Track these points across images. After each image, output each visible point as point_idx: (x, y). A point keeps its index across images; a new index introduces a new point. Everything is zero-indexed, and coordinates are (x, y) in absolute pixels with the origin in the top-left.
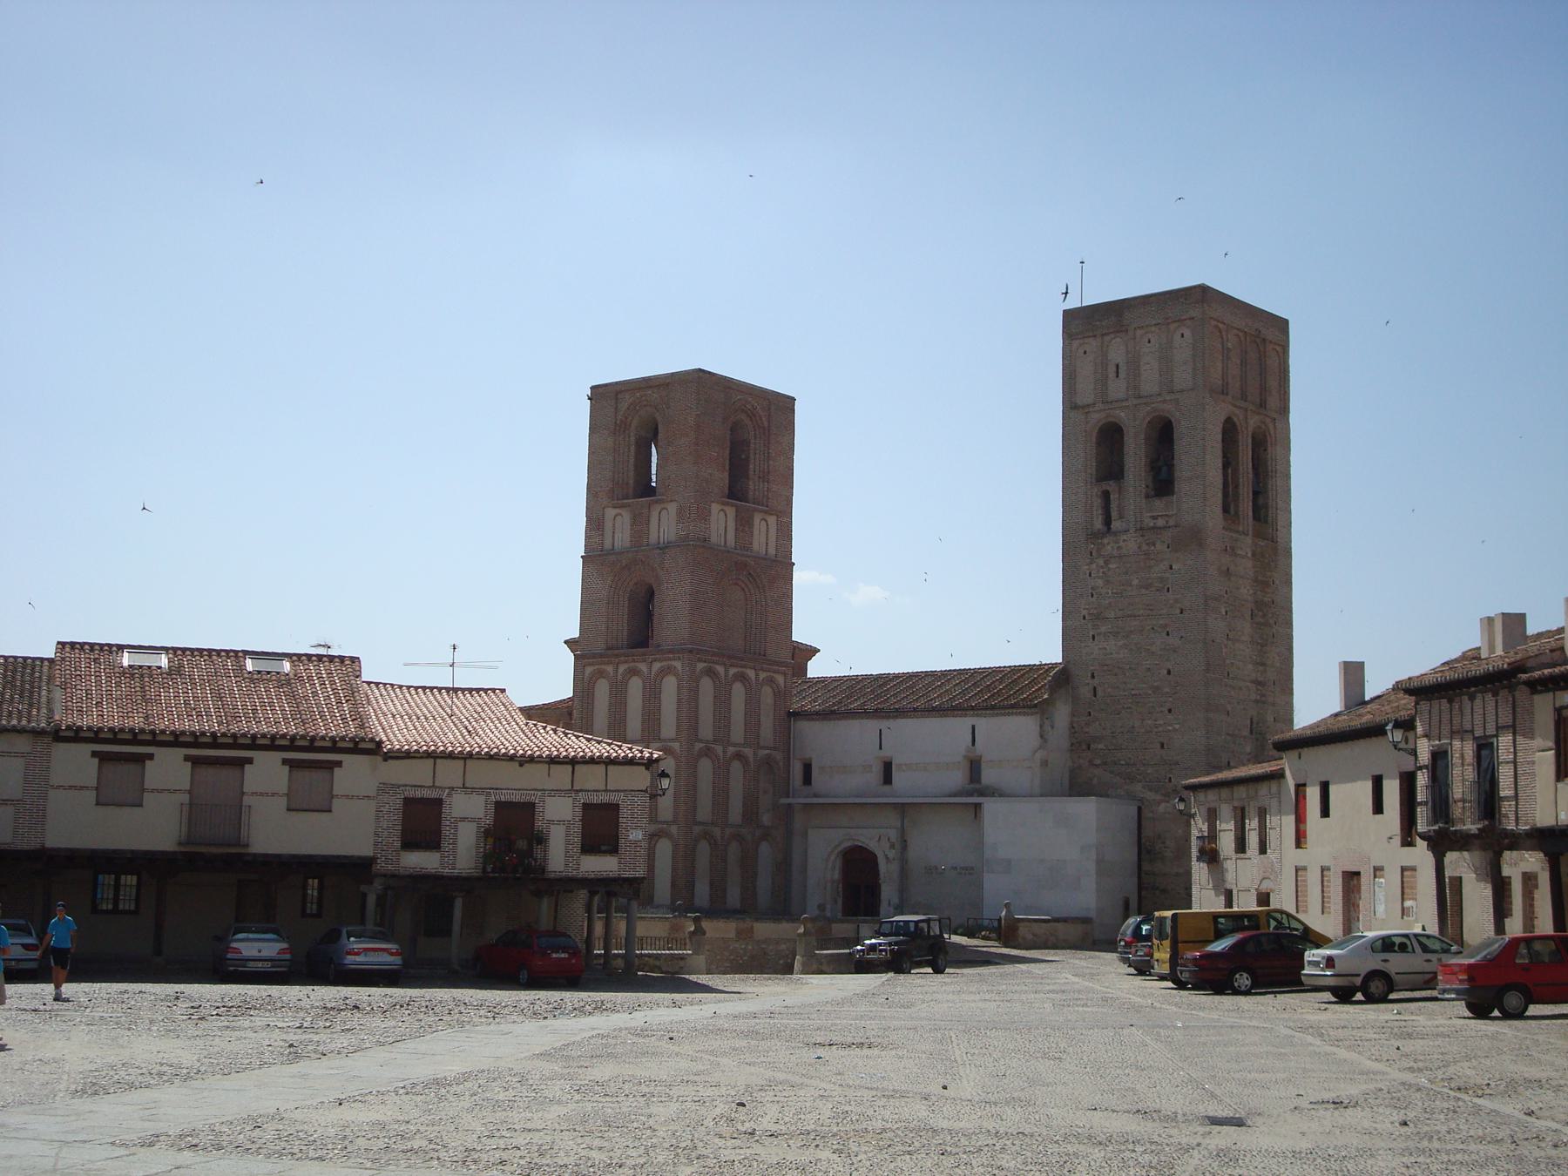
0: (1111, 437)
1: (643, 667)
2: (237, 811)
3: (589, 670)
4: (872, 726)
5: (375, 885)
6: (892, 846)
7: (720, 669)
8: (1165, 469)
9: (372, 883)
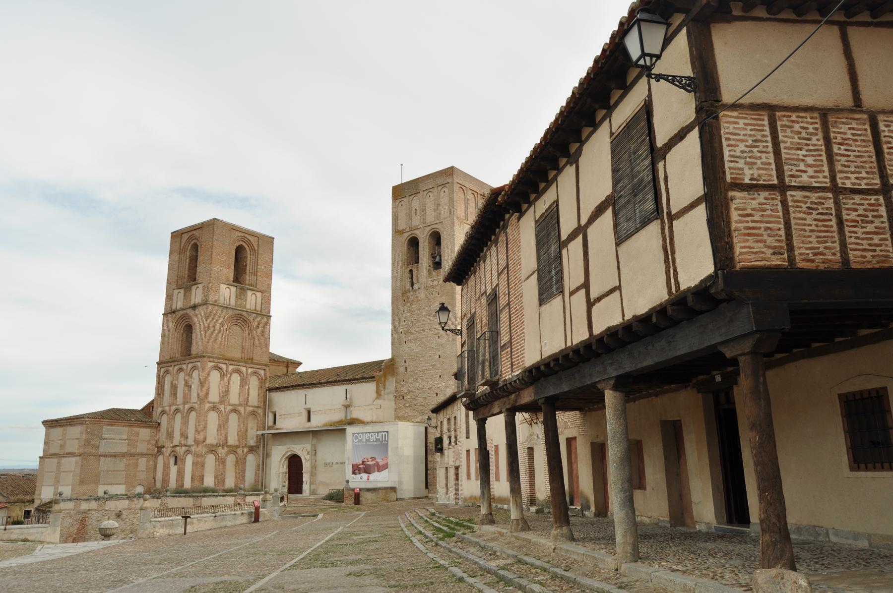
0: (414, 243)
1: (184, 366)
3: (163, 370)
6: (308, 453)
7: (224, 367)
8: (438, 257)
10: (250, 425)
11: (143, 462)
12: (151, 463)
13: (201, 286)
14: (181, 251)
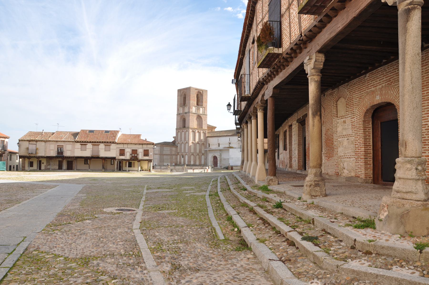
2: (98, 151)
4: (217, 138)
10: (202, 147)
11: (174, 157)
12: (176, 157)
13: (187, 107)
14: (181, 96)
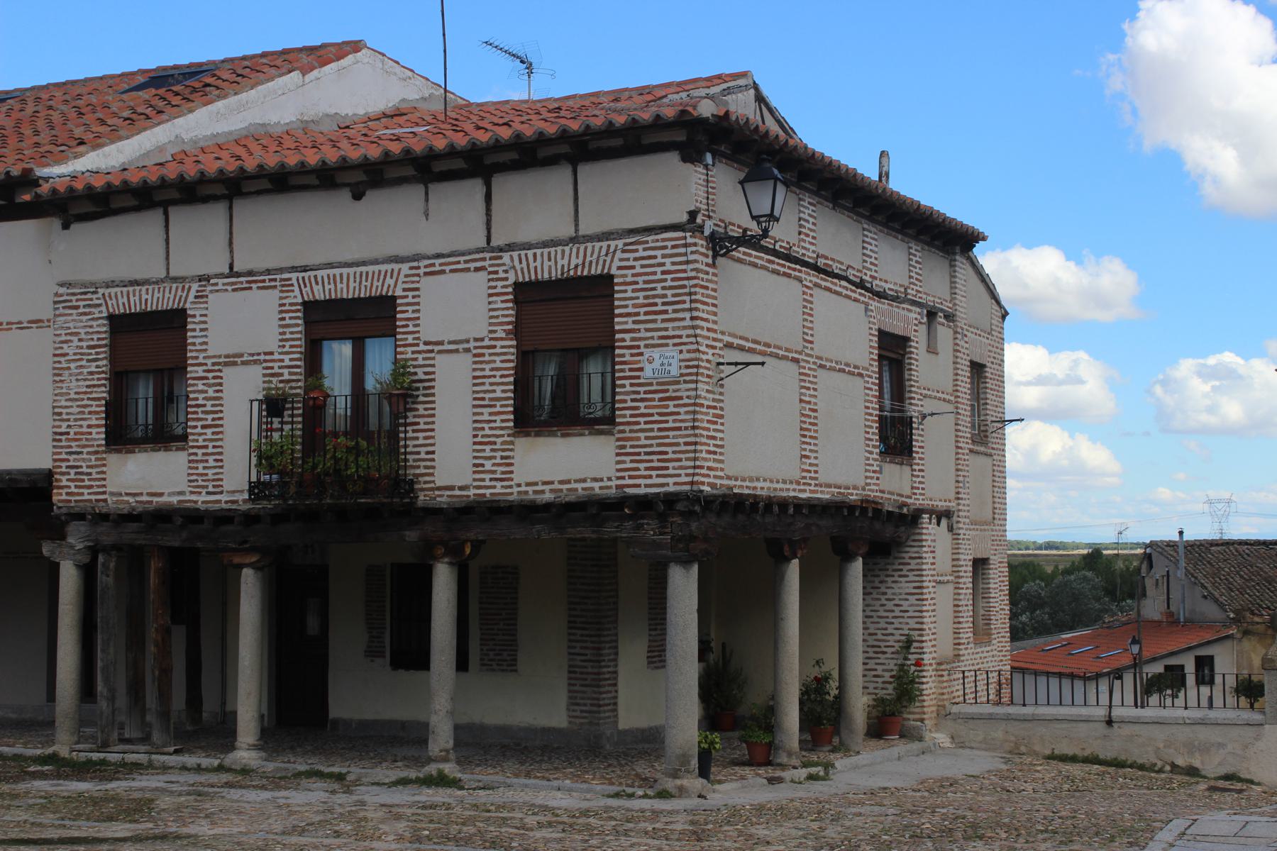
5: (71, 540)
9: (63, 537)
